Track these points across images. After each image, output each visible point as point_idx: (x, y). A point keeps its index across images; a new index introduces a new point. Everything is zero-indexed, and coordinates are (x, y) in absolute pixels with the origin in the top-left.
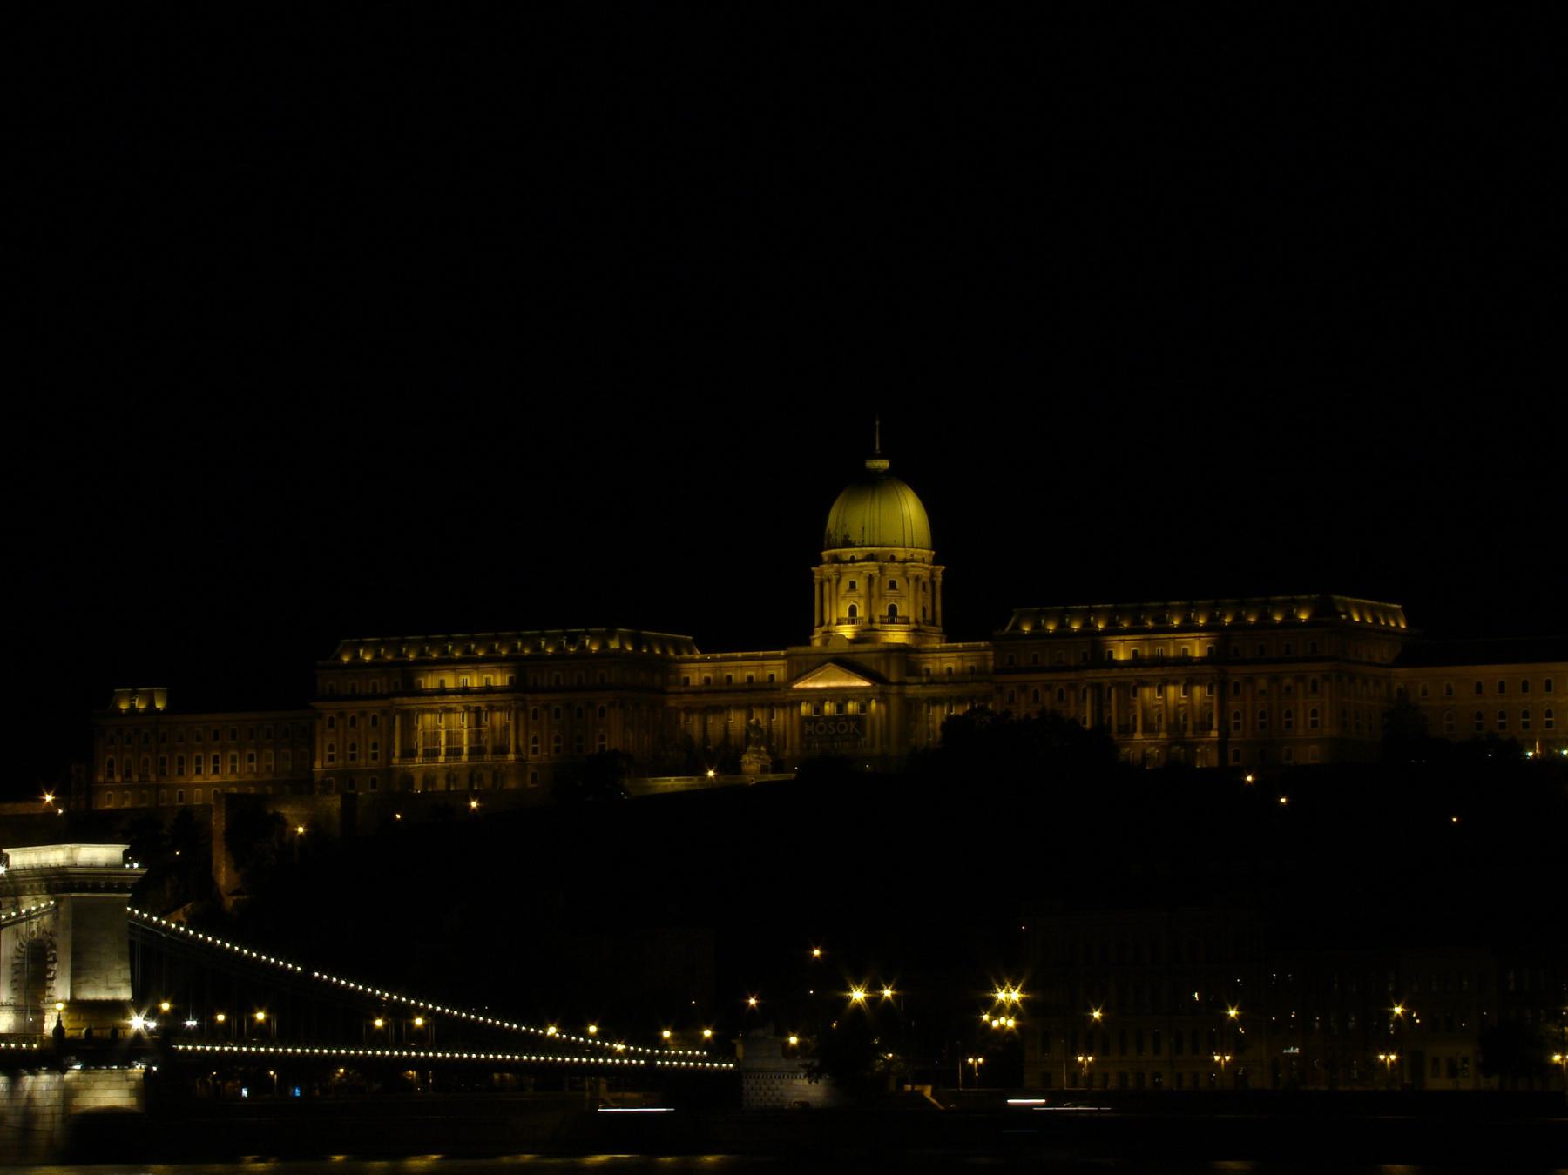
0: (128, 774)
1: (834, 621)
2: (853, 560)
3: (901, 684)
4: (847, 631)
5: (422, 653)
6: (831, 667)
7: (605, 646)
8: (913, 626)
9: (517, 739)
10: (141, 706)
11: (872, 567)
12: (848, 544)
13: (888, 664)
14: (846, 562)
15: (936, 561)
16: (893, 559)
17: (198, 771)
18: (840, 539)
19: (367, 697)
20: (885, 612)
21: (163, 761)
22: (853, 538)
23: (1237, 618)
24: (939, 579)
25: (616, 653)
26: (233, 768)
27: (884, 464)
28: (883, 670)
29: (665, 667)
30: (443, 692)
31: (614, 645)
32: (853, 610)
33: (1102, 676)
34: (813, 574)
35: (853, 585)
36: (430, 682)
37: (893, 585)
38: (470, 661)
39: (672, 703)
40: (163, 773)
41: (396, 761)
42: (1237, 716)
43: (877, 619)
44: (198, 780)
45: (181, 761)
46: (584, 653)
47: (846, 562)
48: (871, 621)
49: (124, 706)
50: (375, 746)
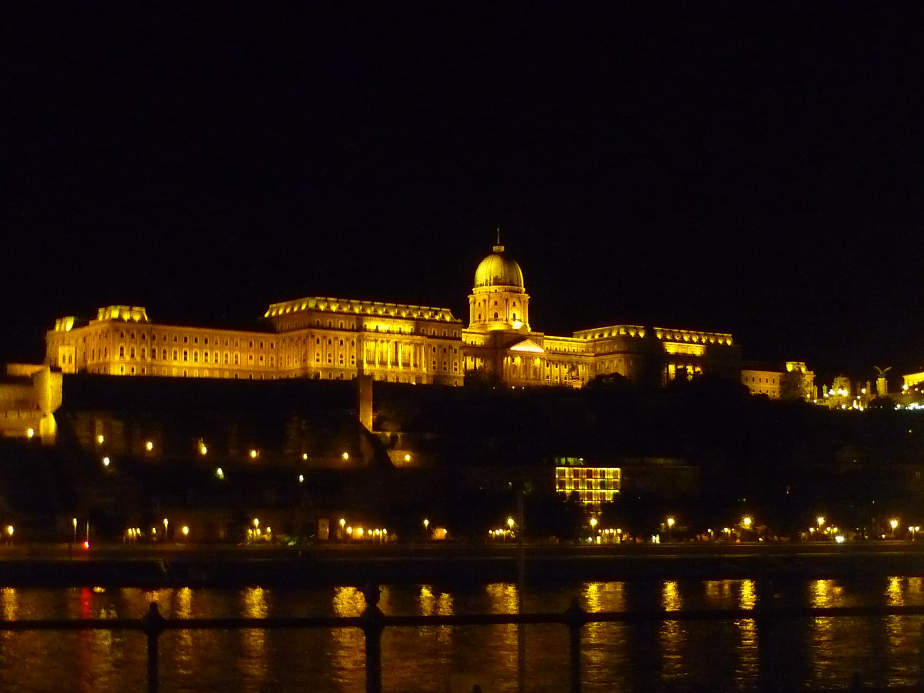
0: (132, 356)
5: (363, 310)
6: (528, 341)
9: (415, 360)
10: (137, 318)
12: (512, 284)
17: (175, 358)
19: (338, 330)
21: (154, 351)
26: (196, 360)
27: (502, 248)
30: (377, 331)
32: (514, 315)
36: (371, 325)
38: (386, 316)
40: (154, 357)
41: (365, 366)
44: (175, 363)
45: (165, 352)
49: (126, 317)
50: (341, 356)
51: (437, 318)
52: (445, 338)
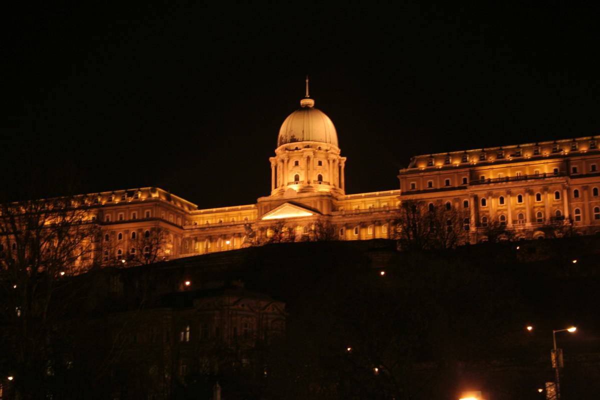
1: (286, 183)
2: (297, 149)
3: (329, 215)
4: (296, 188)
6: (287, 205)
7: (150, 196)
8: (333, 187)
11: (309, 152)
12: (293, 140)
13: (321, 203)
14: (293, 150)
15: (342, 155)
16: (320, 149)
18: (289, 139)
20: (317, 179)
22: (296, 137)
23: (573, 149)
24: (343, 165)
25: (157, 200)
27: (311, 102)
28: (318, 208)
29: (183, 215)
31: (155, 195)
32: (297, 179)
33: (480, 191)
34: (270, 163)
35: (297, 163)
37: (320, 163)
39: (187, 235)
42: (577, 211)
43: (312, 181)
46: (137, 202)
47: (293, 150)
48: (309, 183)
51: (131, 200)
52: (134, 221)
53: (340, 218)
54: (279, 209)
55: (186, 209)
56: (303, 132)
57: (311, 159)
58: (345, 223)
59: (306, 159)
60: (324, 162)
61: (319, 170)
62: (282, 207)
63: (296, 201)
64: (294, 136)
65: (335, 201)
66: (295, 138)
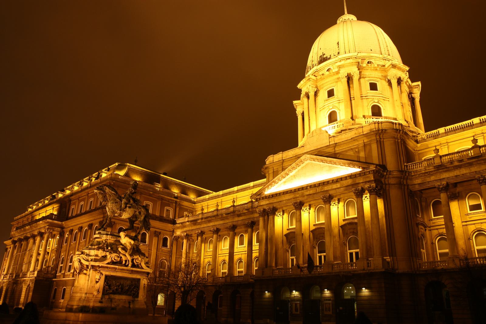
22: (327, 55)
32: (332, 118)
37: (373, 87)
39: (178, 233)
53: (429, 174)
54: (294, 168)
55: (192, 197)
56: (338, 43)
57: (356, 78)
58: (444, 183)
59: (346, 79)
60: (382, 85)
61: (373, 98)
62: (298, 165)
63: (331, 150)
64: (324, 55)
65: (411, 144)
66: (325, 56)
